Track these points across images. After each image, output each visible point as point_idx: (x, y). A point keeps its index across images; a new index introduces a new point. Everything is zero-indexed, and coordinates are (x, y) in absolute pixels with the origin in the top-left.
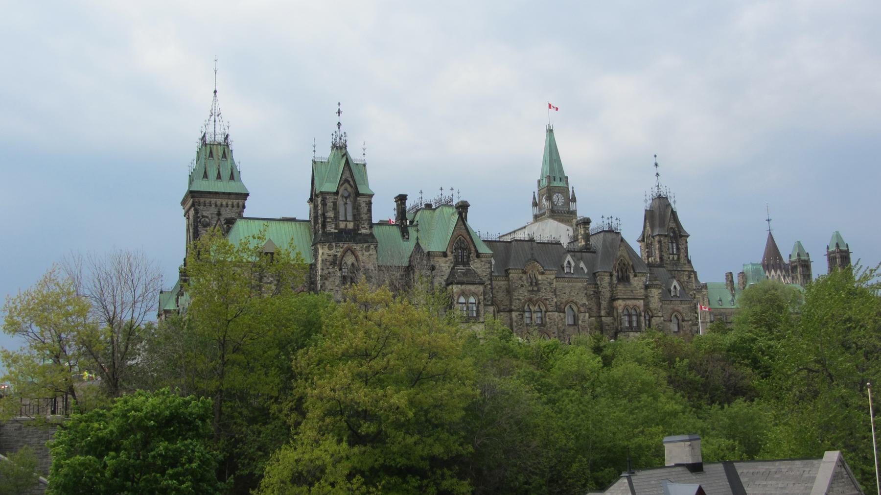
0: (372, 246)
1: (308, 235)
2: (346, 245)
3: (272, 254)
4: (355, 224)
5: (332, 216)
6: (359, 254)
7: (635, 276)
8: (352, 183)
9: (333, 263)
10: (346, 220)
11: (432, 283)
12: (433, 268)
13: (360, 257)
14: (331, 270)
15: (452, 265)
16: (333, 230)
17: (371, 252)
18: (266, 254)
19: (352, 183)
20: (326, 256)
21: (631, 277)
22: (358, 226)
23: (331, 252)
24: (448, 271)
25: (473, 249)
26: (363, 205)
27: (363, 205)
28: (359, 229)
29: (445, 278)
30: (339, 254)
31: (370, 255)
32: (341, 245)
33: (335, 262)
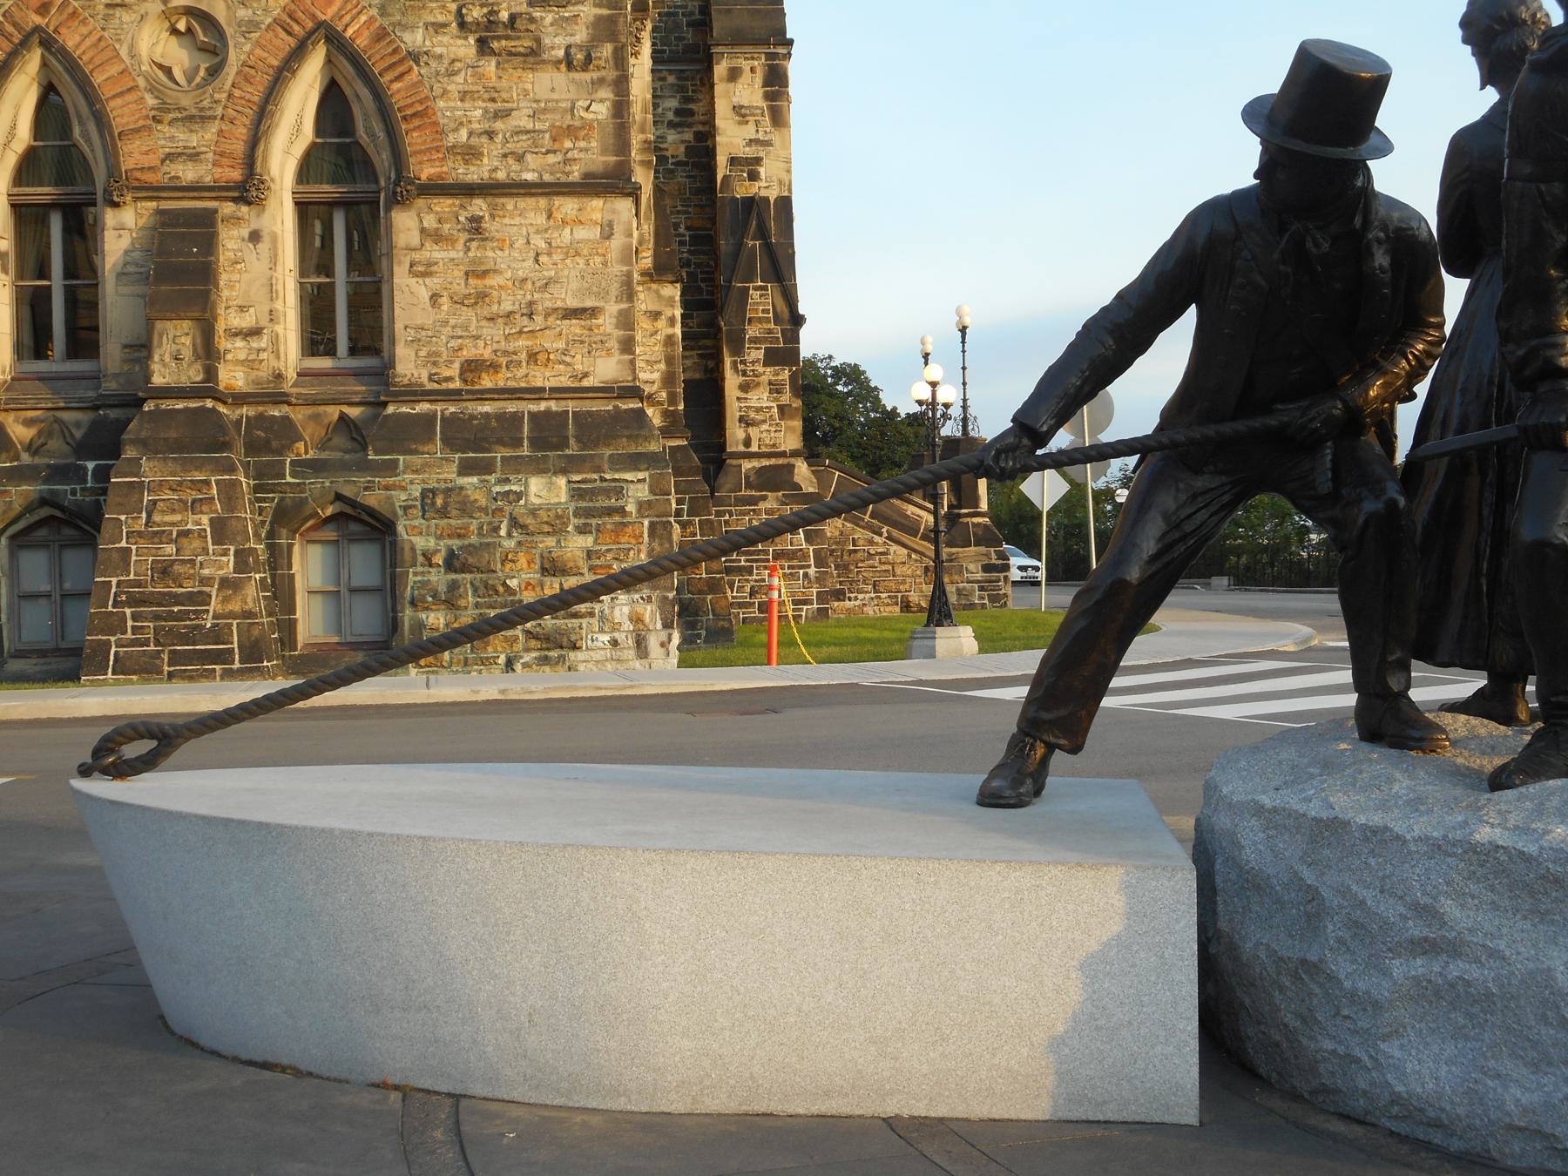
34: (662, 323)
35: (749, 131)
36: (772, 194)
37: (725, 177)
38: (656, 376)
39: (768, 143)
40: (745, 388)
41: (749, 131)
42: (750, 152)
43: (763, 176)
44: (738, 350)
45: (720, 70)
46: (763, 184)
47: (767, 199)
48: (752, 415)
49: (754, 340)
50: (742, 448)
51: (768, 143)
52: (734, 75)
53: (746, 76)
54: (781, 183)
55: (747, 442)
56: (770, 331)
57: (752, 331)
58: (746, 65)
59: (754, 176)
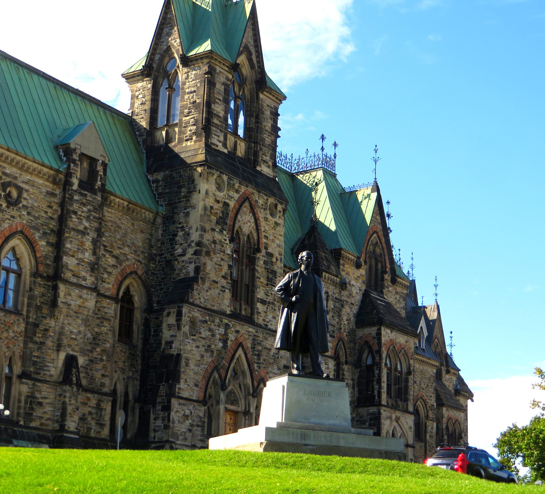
0: (280, 207)
1: (132, 146)
2: (243, 189)
3: (93, 161)
4: (248, 149)
5: (222, 114)
6: (261, 215)
7: (448, 372)
8: (254, 57)
9: (222, 221)
10: (235, 133)
11: (340, 316)
12: (343, 285)
13: (263, 224)
14: (218, 236)
15: (364, 288)
16: (220, 148)
17: (277, 219)
18: (82, 155)
19: (254, 57)
20: (210, 202)
21: (444, 372)
22: (256, 154)
23: (221, 195)
24: (357, 298)
25: (388, 265)
26: (268, 113)
27: (268, 113)
28: (256, 163)
29: (355, 309)
30: (232, 204)
31: (276, 224)
32: (237, 185)
33: (225, 219)
34: (62, 397)
35: (172, 333)
36: (175, 353)
37: (164, 348)
38: (59, 414)
39: (175, 336)
40: (155, 419)
41: (172, 333)
42: (169, 339)
43: (173, 347)
44: (154, 407)
45: (165, 313)
46: (173, 350)
47: (173, 355)
48: (157, 429)
49: (159, 403)
50: (153, 440)
51: (175, 336)
52: (169, 314)
53: (172, 315)
54: (178, 349)
55: (154, 438)
56: (163, 400)
57: (159, 400)
58: (172, 311)
59: (171, 347)
